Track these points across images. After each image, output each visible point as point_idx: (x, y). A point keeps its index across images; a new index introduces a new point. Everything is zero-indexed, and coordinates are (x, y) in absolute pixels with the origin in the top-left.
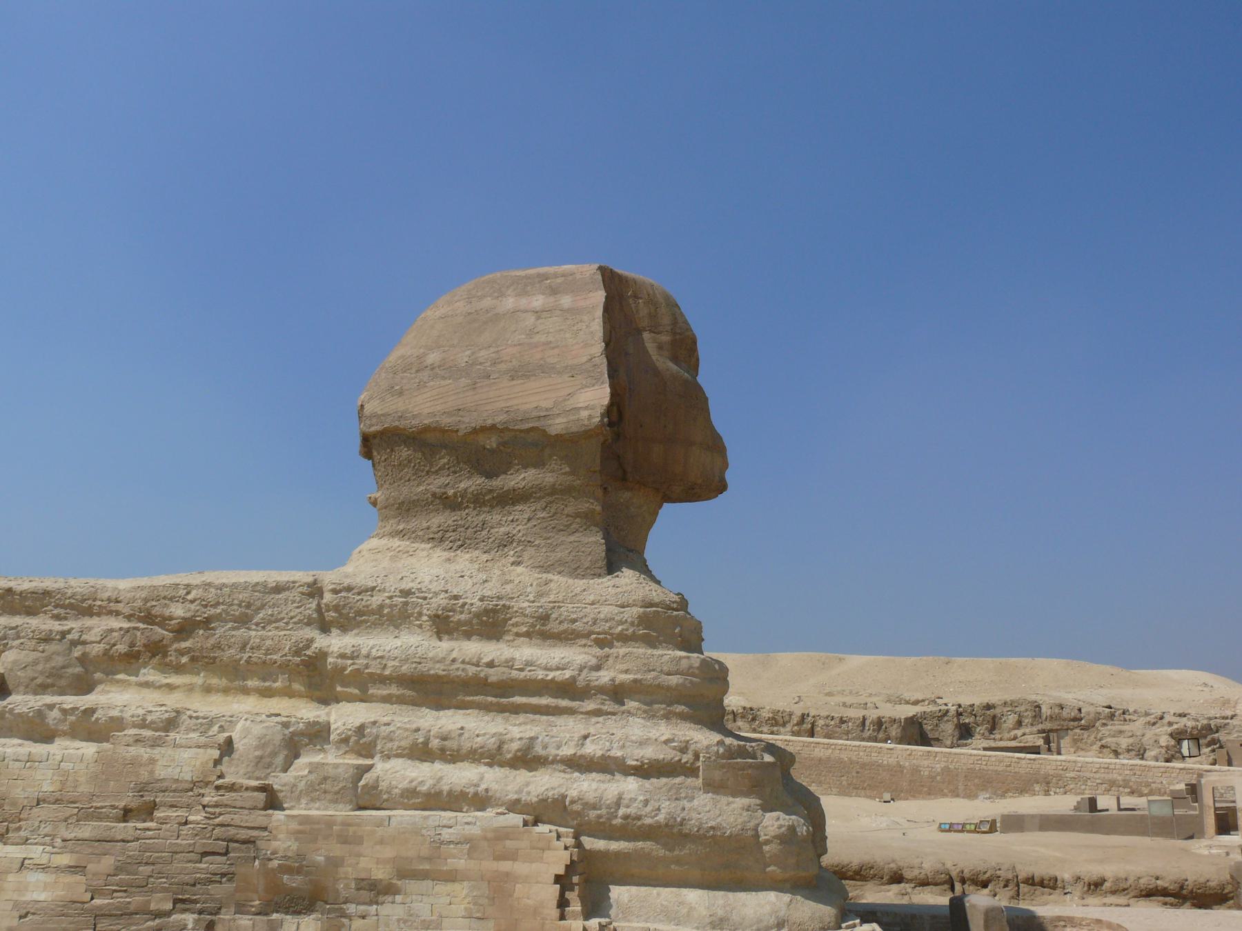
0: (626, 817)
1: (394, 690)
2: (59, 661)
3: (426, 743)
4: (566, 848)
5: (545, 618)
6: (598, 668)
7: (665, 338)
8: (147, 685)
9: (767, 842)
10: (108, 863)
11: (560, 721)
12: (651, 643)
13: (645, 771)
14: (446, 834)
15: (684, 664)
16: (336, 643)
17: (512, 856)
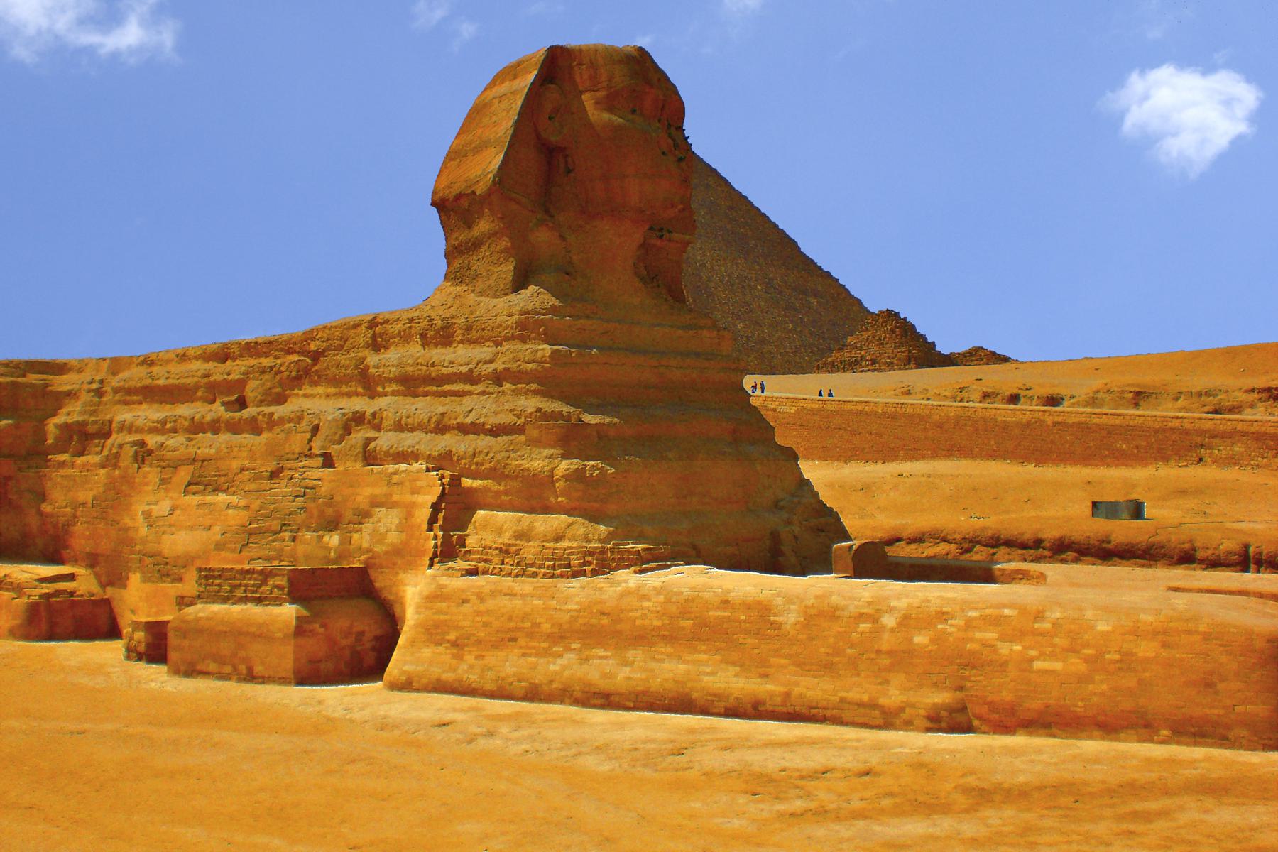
0: (477, 464)
1: (395, 387)
2: (268, 385)
3: (400, 421)
4: (443, 485)
5: (469, 329)
6: (491, 362)
7: (602, 93)
8: (305, 396)
9: (558, 480)
10: (256, 504)
11: (466, 400)
12: (523, 339)
13: (495, 431)
14: (395, 478)
15: (540, 354)
16: (372, 359)
17: (415, 491)
